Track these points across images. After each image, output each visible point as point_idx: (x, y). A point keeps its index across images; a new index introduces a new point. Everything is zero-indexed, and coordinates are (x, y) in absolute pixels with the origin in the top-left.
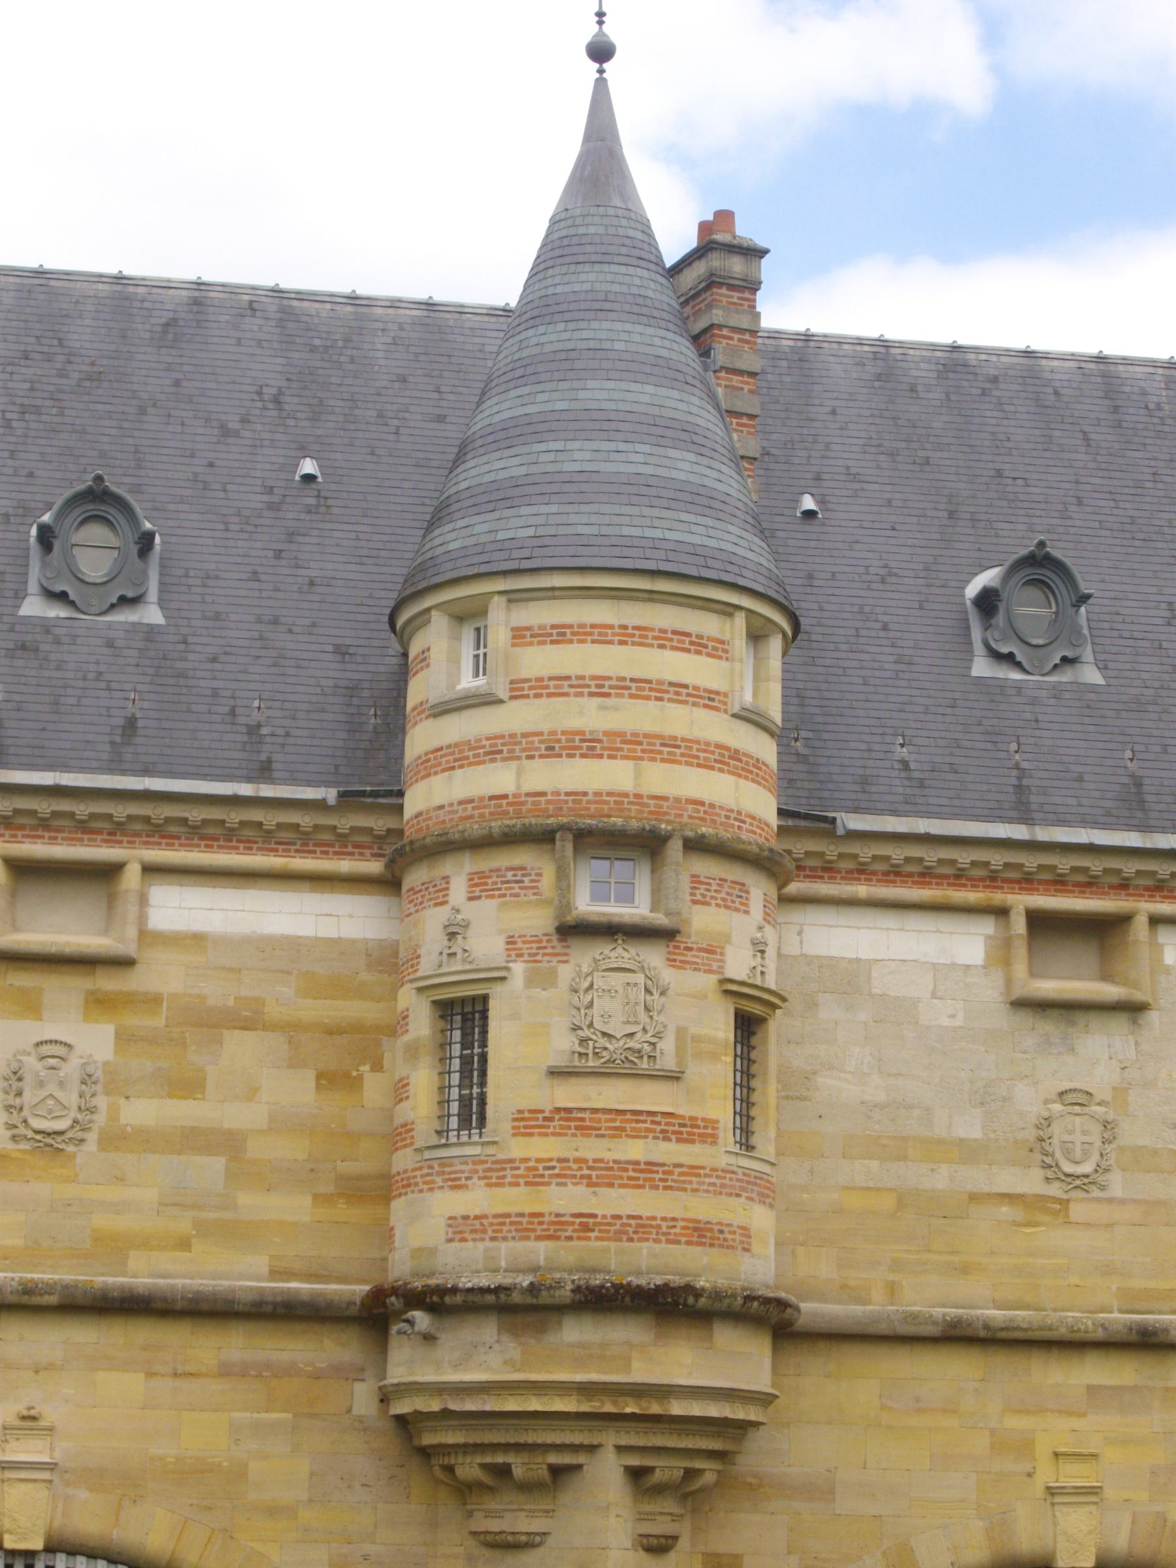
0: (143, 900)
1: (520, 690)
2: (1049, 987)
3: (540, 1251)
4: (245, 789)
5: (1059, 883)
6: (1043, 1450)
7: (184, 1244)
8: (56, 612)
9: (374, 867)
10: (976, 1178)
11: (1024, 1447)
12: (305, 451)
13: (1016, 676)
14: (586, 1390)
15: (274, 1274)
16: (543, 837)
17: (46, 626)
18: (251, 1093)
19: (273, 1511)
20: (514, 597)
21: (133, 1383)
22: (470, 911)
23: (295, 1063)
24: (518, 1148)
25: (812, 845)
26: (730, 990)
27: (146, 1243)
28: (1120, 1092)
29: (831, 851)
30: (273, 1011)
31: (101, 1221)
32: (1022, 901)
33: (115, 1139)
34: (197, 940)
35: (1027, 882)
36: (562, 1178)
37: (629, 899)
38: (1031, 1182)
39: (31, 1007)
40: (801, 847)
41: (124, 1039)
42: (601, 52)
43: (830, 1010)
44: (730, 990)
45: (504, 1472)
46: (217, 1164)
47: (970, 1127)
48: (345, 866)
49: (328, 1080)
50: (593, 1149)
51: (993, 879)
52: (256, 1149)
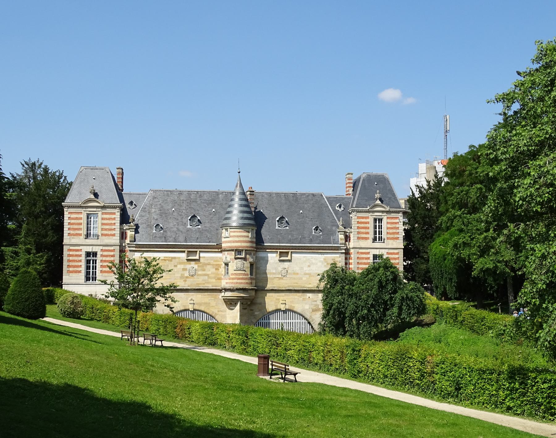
0: (199, 254)
1: (231, 237)
2: (282, 258)
3: (233, 285)
4: (208, 244)
5: (283, 249)
6: (280, 300)
7: (204, 284)
8: (191, 227)
9: (220, 250)
10: (274, 276)
11: (279, 300)
12: (213, 208)
13: (280, 228)
14: (237, 297)
15: (212, 286)
16: (233, 250)
17: (190, 229)
18: (210, 271)
19: (212, 306)
20: (230, 229)
21: (200, 296)
22: (227, 256)
23: (213, 268)
24: (231, 277)
25: (260, 246)
26: (250, 262)
27: (201, 284)
28: (288, 268)
29: (261, 247)
30: (211, 263)
31: (197, 282)
32: (279, 251)
33: (198, 275)
34: (204, 257)
35: (280, 249)
36: (235, 279)
37: (240, 254)
38: (280, 276)
39: (190, 264)
40: (259, 247)
41: (198, 266)
42: (239, 172)
43: (261, 261)
44: (250, 262)
45: (231, 303)
46: (207, 277)
47: (274, 271)
48: (217, 250)
49: (217, 269)
50: (237, 277)
51: (277, 249)
52: (210, 276)
